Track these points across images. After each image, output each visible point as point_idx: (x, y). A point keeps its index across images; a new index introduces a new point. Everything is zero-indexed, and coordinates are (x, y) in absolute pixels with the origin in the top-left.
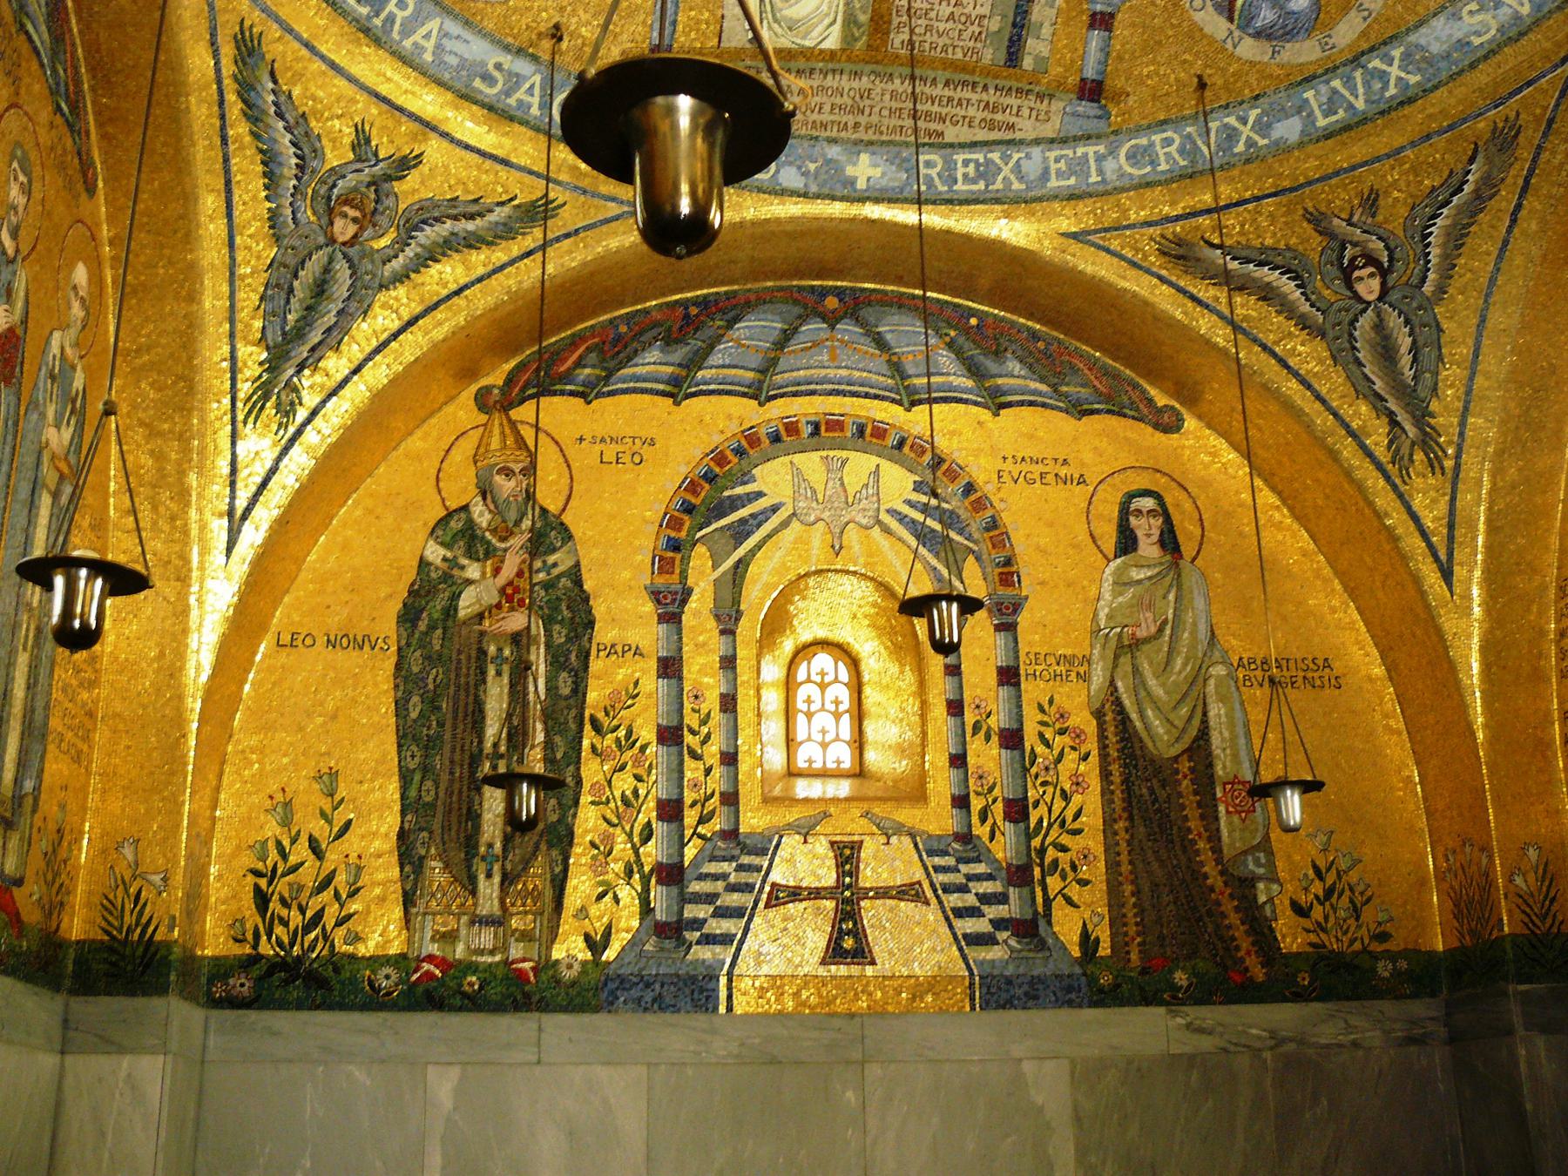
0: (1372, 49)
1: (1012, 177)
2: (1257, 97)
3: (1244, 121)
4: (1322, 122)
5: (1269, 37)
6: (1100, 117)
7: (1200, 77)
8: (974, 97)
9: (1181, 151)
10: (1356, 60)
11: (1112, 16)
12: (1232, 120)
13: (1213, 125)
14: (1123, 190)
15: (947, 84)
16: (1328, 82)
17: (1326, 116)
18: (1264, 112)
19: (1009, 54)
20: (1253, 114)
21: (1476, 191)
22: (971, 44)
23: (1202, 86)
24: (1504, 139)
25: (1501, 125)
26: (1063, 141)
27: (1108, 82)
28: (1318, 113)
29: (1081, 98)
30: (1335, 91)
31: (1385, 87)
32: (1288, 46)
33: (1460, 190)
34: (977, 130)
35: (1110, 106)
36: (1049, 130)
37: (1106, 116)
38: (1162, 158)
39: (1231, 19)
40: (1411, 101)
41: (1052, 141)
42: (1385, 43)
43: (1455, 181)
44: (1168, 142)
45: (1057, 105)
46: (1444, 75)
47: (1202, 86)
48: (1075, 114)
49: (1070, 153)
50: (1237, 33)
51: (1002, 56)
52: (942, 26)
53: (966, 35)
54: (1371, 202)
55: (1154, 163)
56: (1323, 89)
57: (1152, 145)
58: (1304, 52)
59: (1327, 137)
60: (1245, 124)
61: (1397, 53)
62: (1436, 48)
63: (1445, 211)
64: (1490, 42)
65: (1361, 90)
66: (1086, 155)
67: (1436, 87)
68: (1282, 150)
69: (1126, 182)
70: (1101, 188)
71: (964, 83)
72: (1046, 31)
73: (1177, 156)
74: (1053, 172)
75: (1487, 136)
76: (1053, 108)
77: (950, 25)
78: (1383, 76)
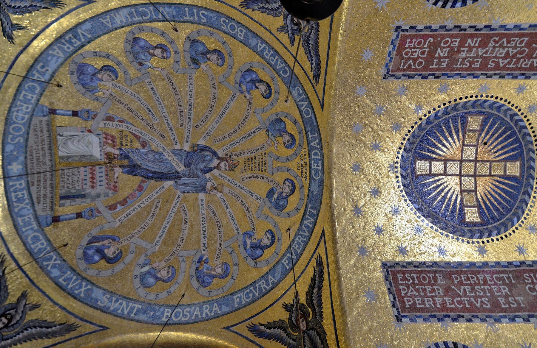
0: (88, 281)
1: (19, 208)
2: (64, 260)
3: (55, 260)
4: (60, 280)
5: (84, 255)
6: (47, 224)
7: (67, 244)
8: (48, 191)
9: (40, 249)
10: (83, 278)
11: (81, 217)
12: (55, 257)
13: (52, 254)
14: (21, 238)
15: (51, 184)
16: (74, 275)
17: (63, 280)
18: (59, 265)
19: (64, 197)
20: (59, 262)
21: (49, 332)
22: (66, 187)
23: (65, 245)
24: (70, 328)
25: (75, 324)
26: (36, 217)
27: (60, 223)
28: (63, 278)
29: (53, 218)
30: (72, 278)
31: (77, 290)
32: (83, 261)
33: (48, 328)
34: (36, 194)
35: (52, 226)
36: (40, 213)
37: (48, 225)
38: (36, 245)
39: (87, 244)
40: (75, 298)
41: (36, 214)
42: (91, 282)
43: (51, 325)
44: (42, 244)
45: (49, 212)
46: (86, 301)
47: (65, 245)
48: (47, 218)
49: (32, 220)
50: (83, 247)
51: (63, 195)
52: (70, 179)
53: (68, 185)
54: (36, 306)
55: (34, 243)
56: (72, 275)
57: (40, 240)
58: (82, 265)
59: (56, 284)
60: (55, 261)
61: (89, 287)
62: (93, 295)
63: (38, 329)
64: (100, 306)
65: (74, 284)
66: (33, 224)
67: (81, 302)
68: (48, 274)
69: (24, 238)
70: (20, 232)
71: (52, 188)
72: (73, 203)
73: (38, 248)
74: (24, 218)
75: (70, 323)
76: (48, 212)
77: (71, 181)
78: (81, 287)
